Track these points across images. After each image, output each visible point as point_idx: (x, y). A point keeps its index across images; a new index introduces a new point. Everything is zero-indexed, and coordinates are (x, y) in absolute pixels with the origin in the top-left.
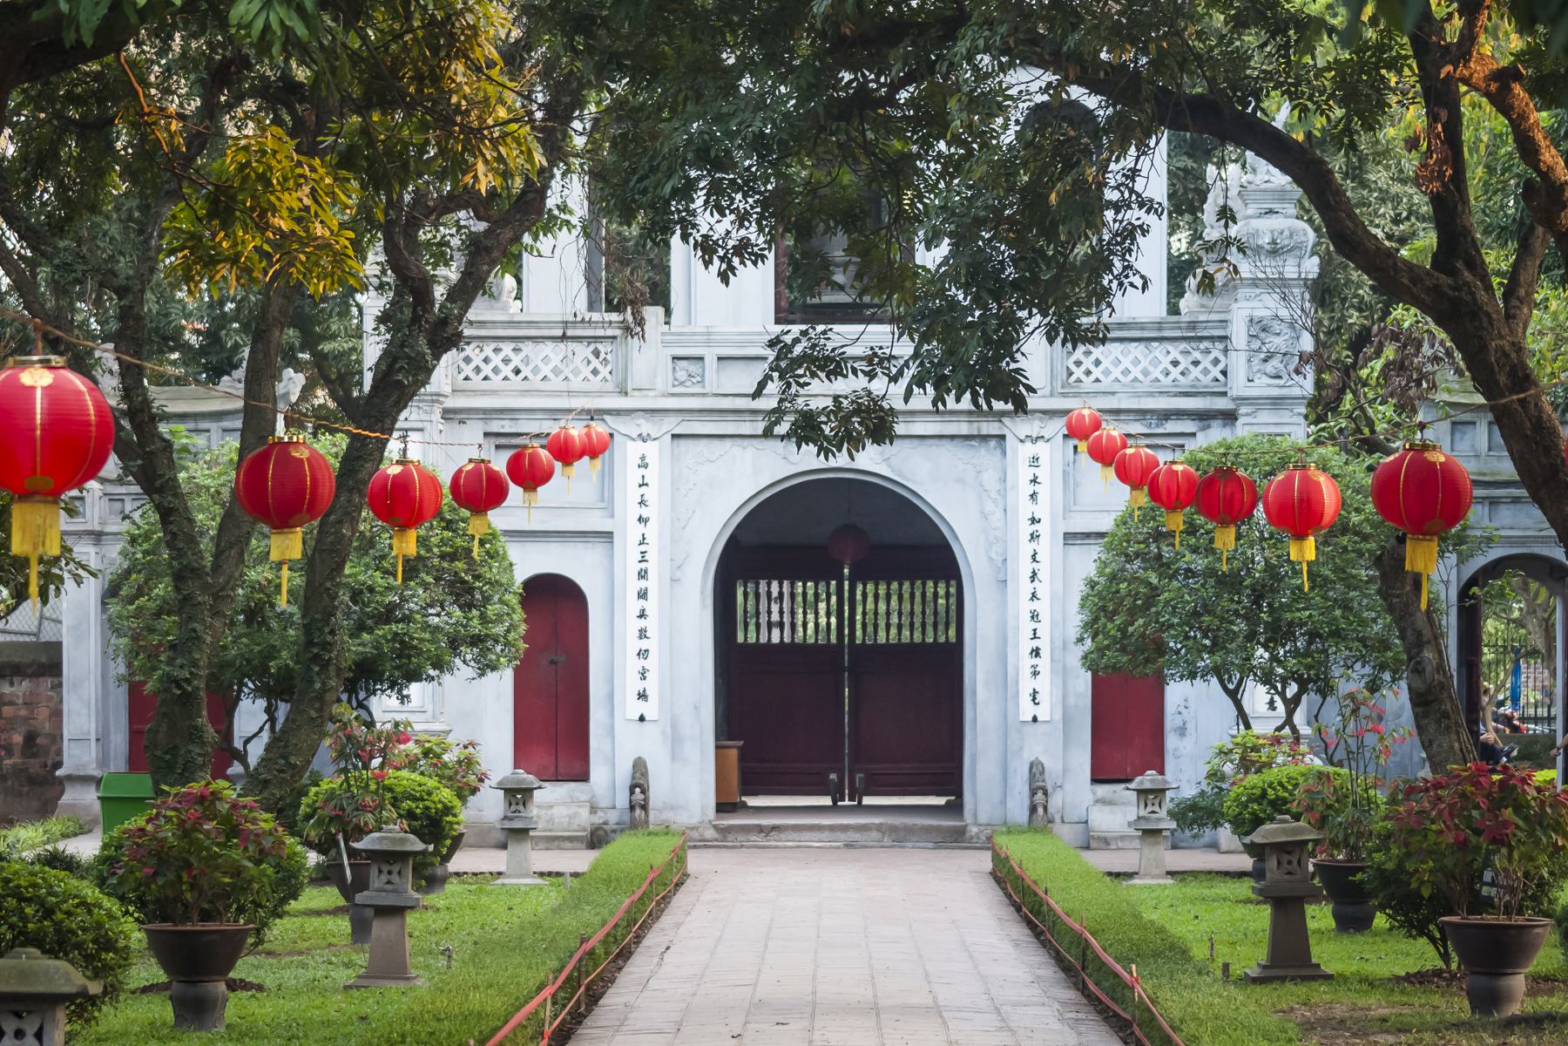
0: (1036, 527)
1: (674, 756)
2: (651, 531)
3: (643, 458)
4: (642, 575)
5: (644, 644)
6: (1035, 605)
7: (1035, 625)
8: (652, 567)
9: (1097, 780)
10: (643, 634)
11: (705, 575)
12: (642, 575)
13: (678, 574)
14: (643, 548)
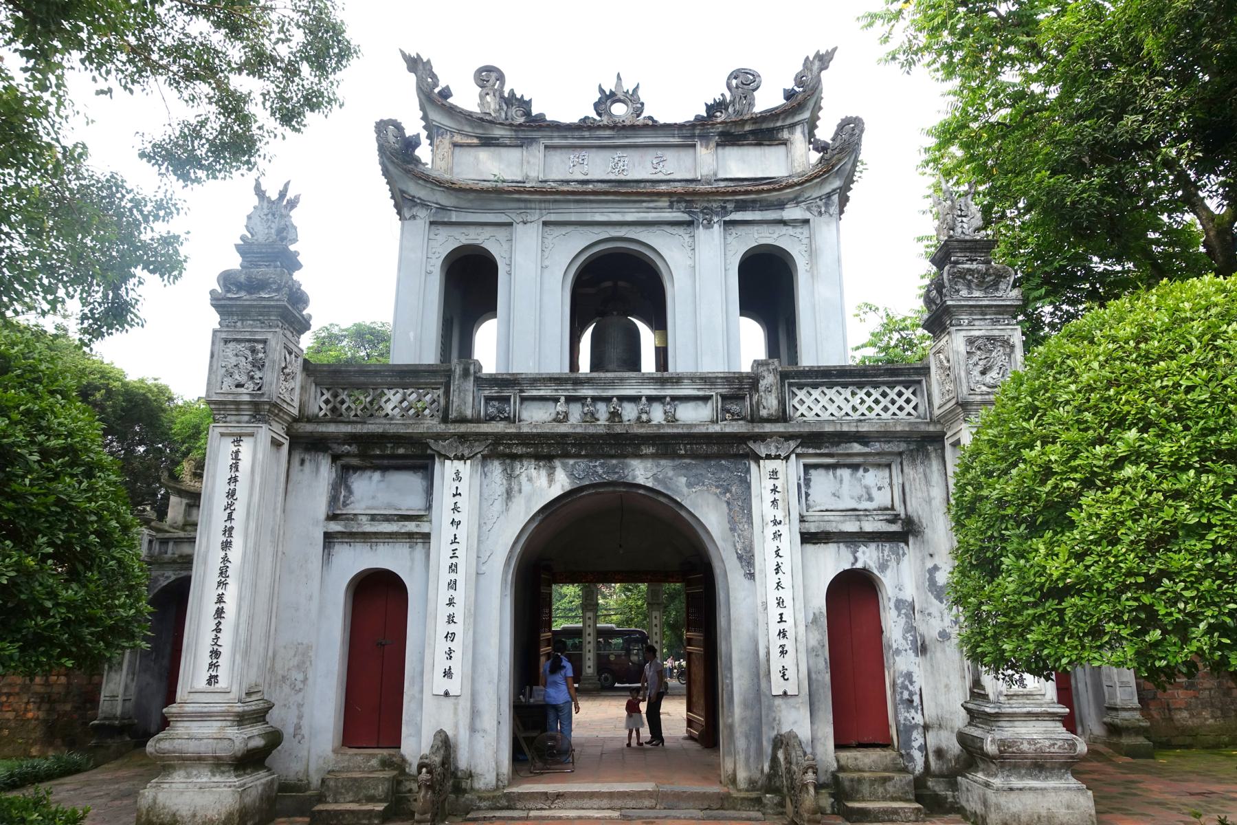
0: (779, 527)
1: (473, 729)
2: (462, 532)
3: (457, 473)
4: (453, 568)
5: (452, 628)
6: (781, 593)
7: (781, 611)
8: (461, 562)
9: (838, 747)
10: (451, 619)
11: (505, 572)
12: (453, 568)
13: (484, 568)
14: (455, 546)
